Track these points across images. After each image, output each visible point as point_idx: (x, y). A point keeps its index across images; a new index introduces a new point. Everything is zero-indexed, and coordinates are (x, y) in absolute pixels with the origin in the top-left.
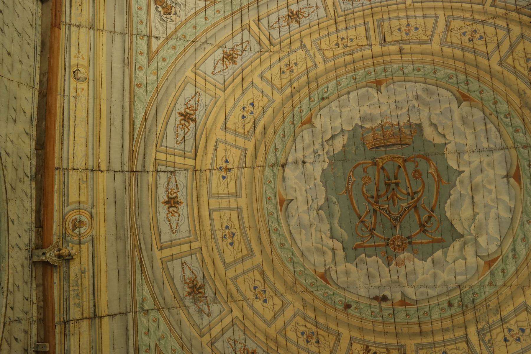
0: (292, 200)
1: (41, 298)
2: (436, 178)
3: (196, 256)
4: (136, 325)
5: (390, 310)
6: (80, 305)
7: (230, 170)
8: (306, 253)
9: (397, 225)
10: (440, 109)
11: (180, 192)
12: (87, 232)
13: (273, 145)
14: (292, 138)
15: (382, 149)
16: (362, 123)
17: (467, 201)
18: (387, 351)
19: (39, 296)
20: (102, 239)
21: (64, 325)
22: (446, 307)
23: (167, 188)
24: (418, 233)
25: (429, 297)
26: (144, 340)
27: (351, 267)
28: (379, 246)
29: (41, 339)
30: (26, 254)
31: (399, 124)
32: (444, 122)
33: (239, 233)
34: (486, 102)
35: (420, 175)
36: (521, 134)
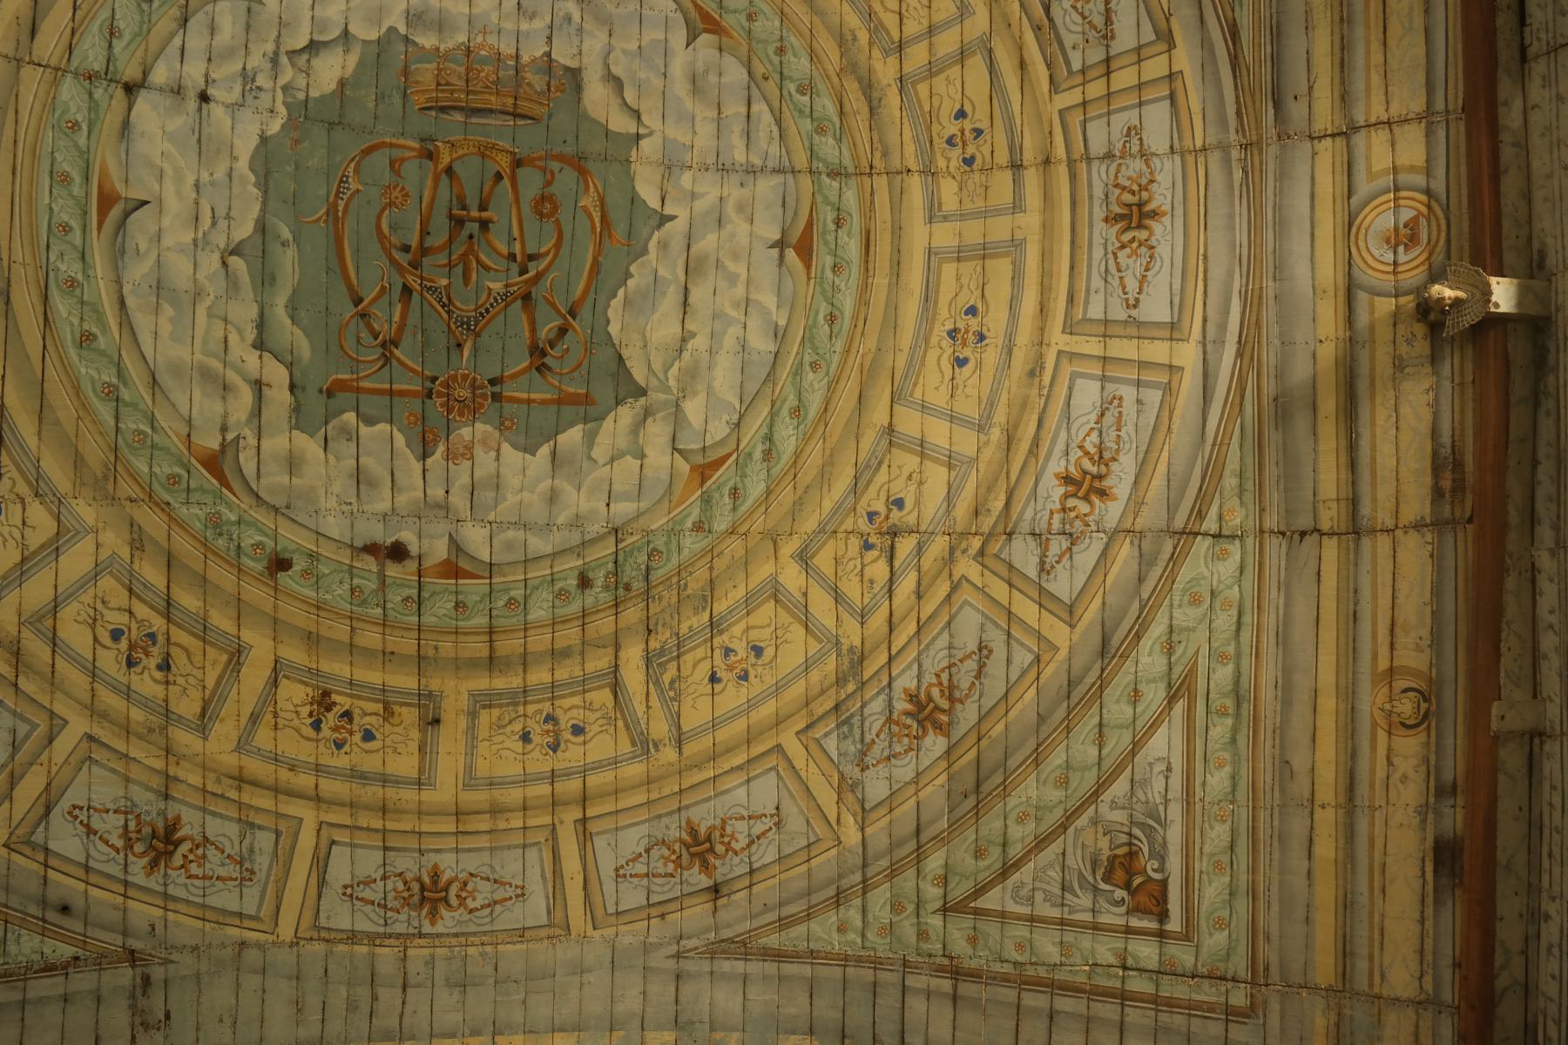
0: (146, 203)
2: (598, 225)
5: (410, 587)
8: (166, 380)
10: (640, 40)
15: (458, 117)
17: (671, 298)
18: (385, 709)
22: (573, 589)
24: (522, 372)
25: (529, 557)
27: (310, 446)
28: (402, 393)
31: (517, 57)
32: (642, 75)
34: (761, 45)
35: (555, 209)
36: (831, 141)
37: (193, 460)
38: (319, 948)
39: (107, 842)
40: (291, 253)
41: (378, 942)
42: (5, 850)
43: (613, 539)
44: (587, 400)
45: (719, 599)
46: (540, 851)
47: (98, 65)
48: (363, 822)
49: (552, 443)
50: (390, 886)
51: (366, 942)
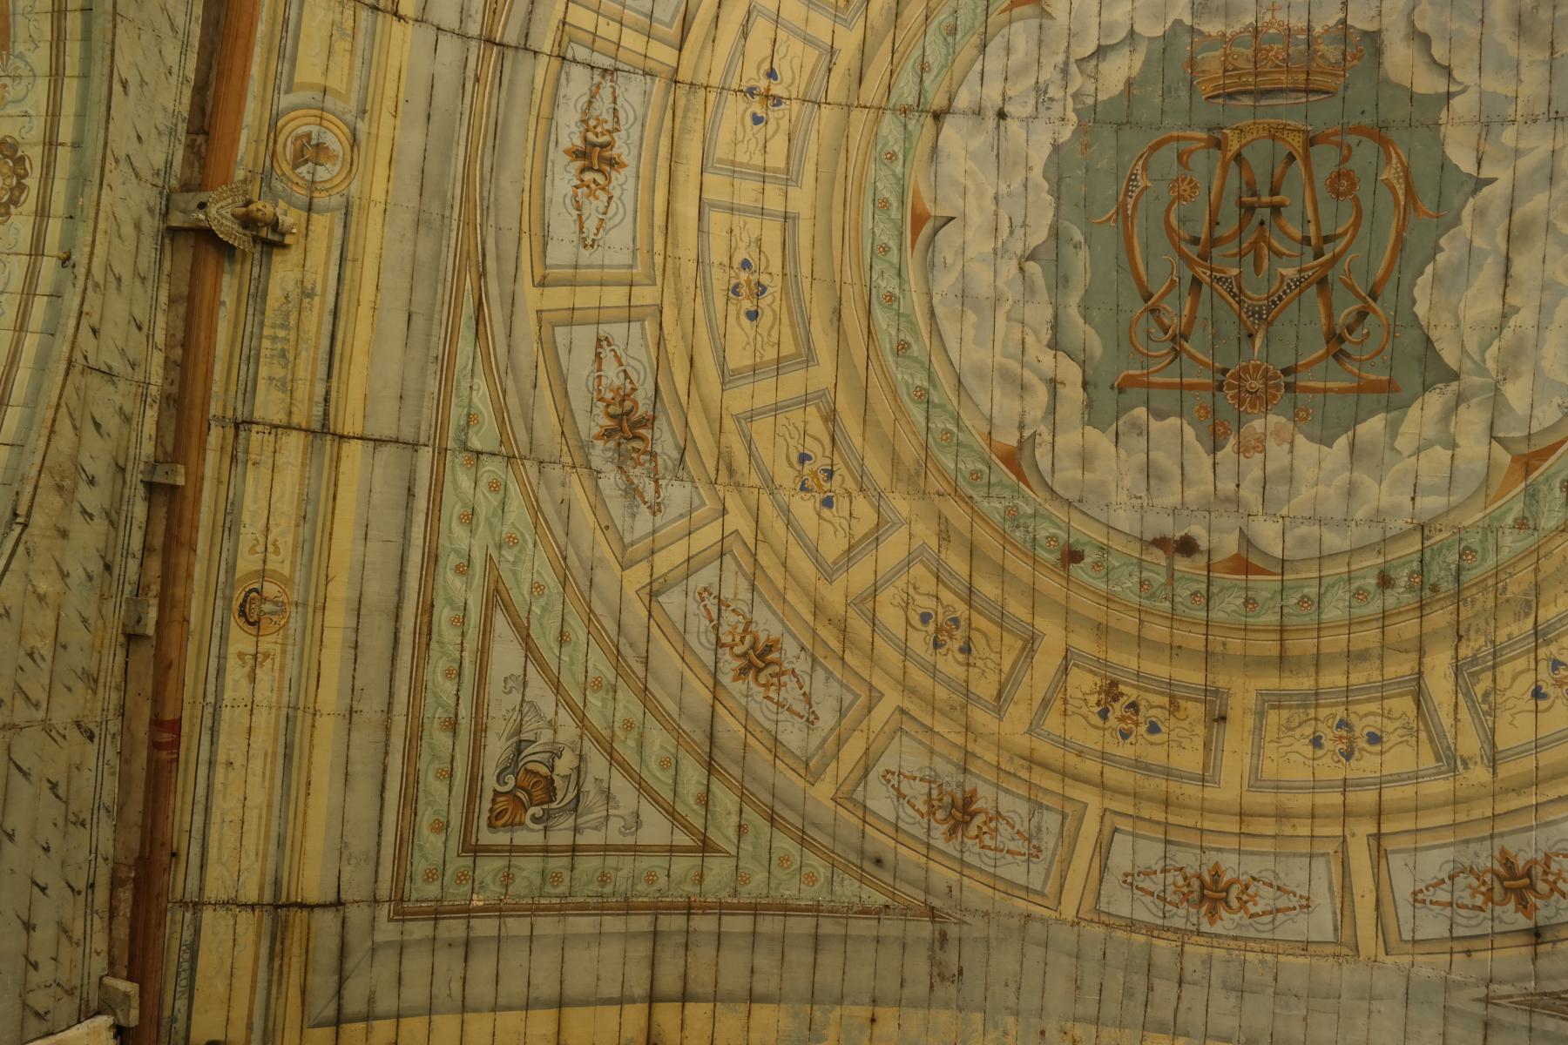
1: (180, 336)
2: (1402, 198)
3: (643, 328)
4: (439, 489)
6: (287, 386)
7: (778, 101)
8: (970, 382)
9: (1257, 331)
11: (623, 134)
12: (336, 182)
13: (917, 53)
14: (976, 40)
15: (1247, 101)
16: (1196, 20)
17: (1489, 271)
18: (1171, 703)
19: (172, 332)
20: (376, 213)
21: (233, 431)
22: (1372, 589)
23: (584, 113)
24: (1319, 359)
25: (1324, 553)
26: (456, 536)
27: (1101, 441)
28: (1191, 387)
29: (165, 453)
30: (152, 196)
31: (1309, 29)
33: (779, 289)
35: (1353, 185)
37: (994, 457)
38: (1099, 931)
39: (913, 807)
40: (1083, 253)
41: (1156, 933)
42: (832, 804)
43: (1418, 537)
44: (1390, 386)
45: (1545, 605)
46: (1328, 862)
47: (911, 100)
48: (1145, 813)
49: (1350, 434)
50: (1170, 879)
51: (1144, 931)
